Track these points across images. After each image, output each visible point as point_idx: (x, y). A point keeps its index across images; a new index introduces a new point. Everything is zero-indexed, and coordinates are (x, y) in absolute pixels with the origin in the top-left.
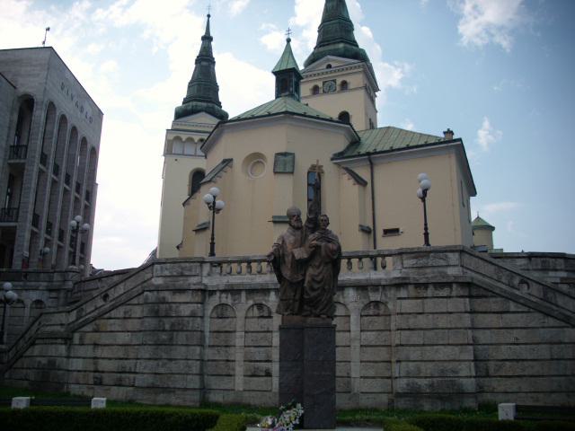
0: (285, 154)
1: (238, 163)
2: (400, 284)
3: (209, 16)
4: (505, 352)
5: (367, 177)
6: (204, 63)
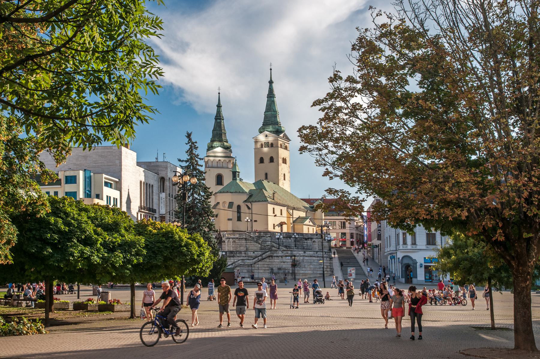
0: (231, 202)
1: (221, 203)
2: (237, 238)
3: (219, 93)
4: (251, 248)
5: (251, 208)
6: (218, 121)
